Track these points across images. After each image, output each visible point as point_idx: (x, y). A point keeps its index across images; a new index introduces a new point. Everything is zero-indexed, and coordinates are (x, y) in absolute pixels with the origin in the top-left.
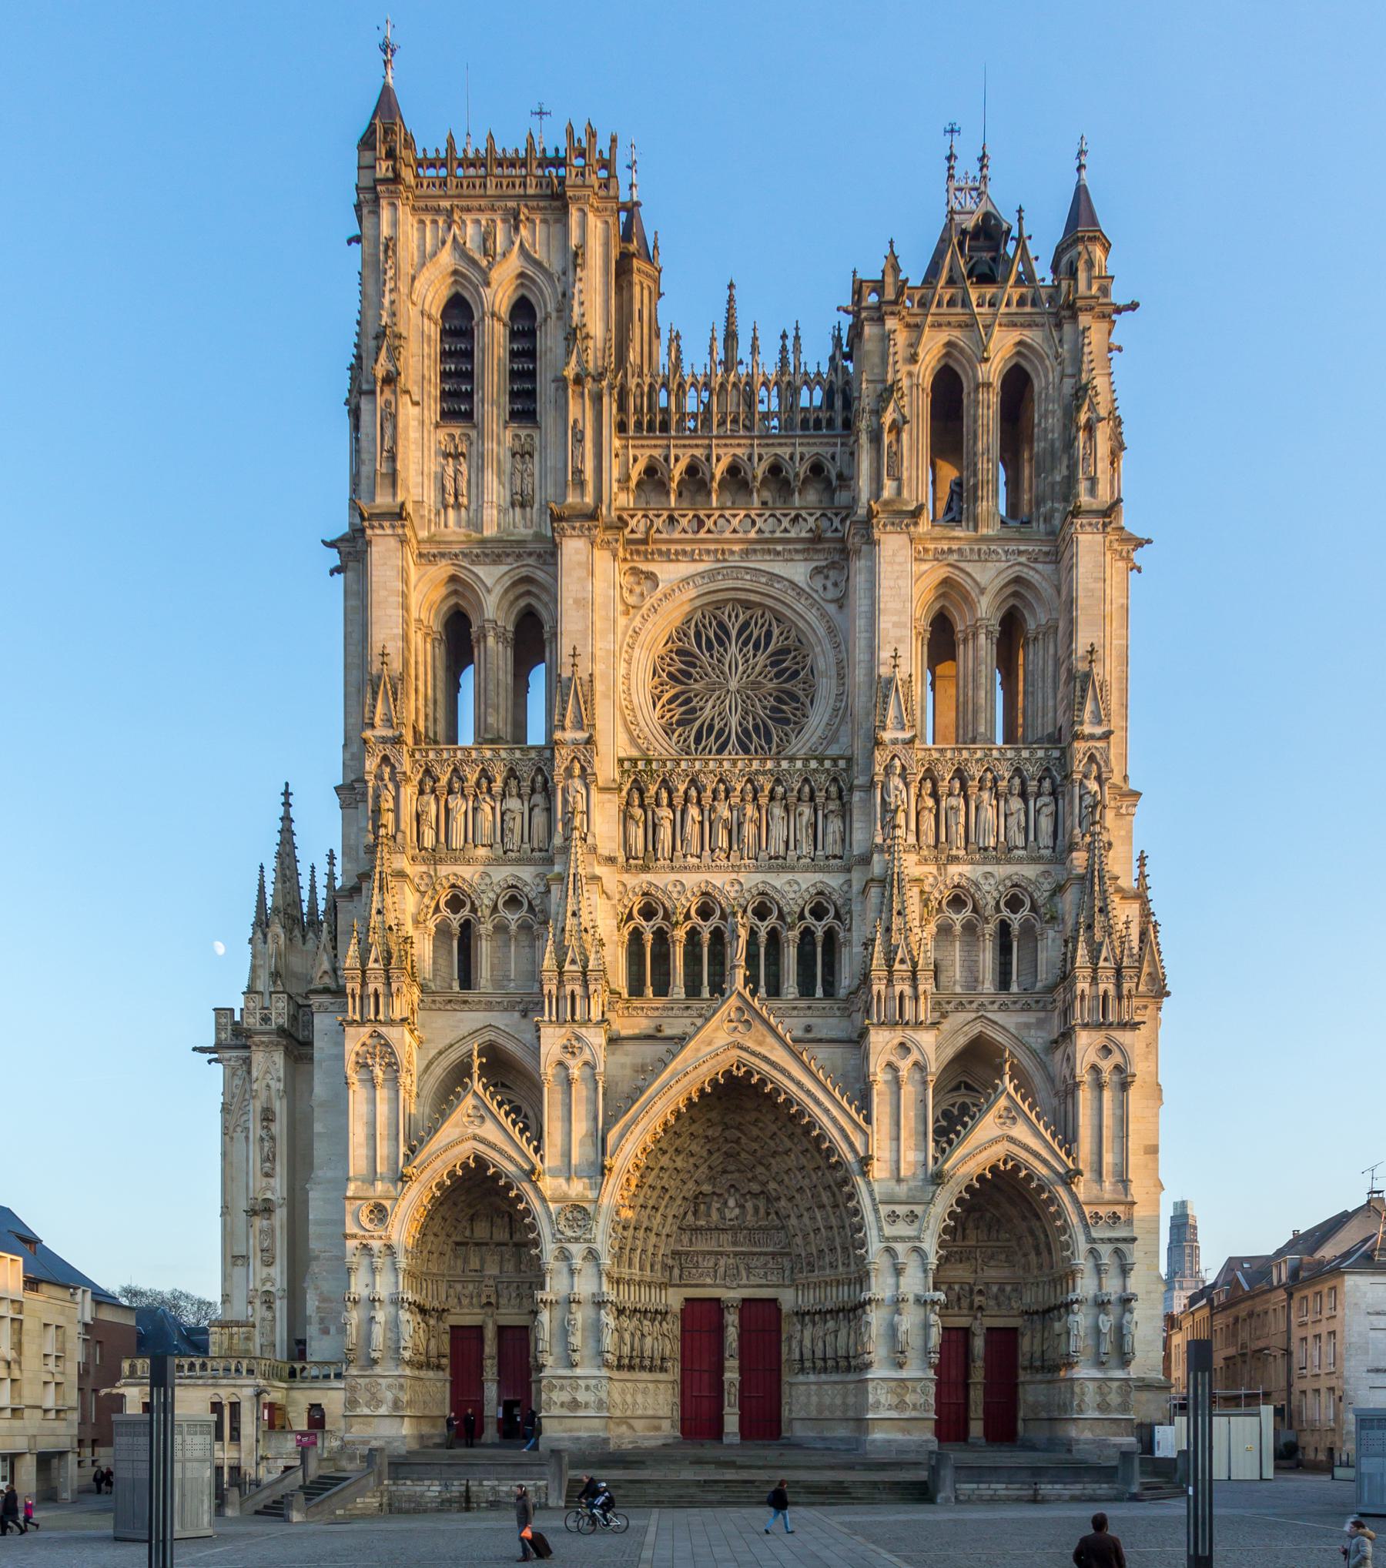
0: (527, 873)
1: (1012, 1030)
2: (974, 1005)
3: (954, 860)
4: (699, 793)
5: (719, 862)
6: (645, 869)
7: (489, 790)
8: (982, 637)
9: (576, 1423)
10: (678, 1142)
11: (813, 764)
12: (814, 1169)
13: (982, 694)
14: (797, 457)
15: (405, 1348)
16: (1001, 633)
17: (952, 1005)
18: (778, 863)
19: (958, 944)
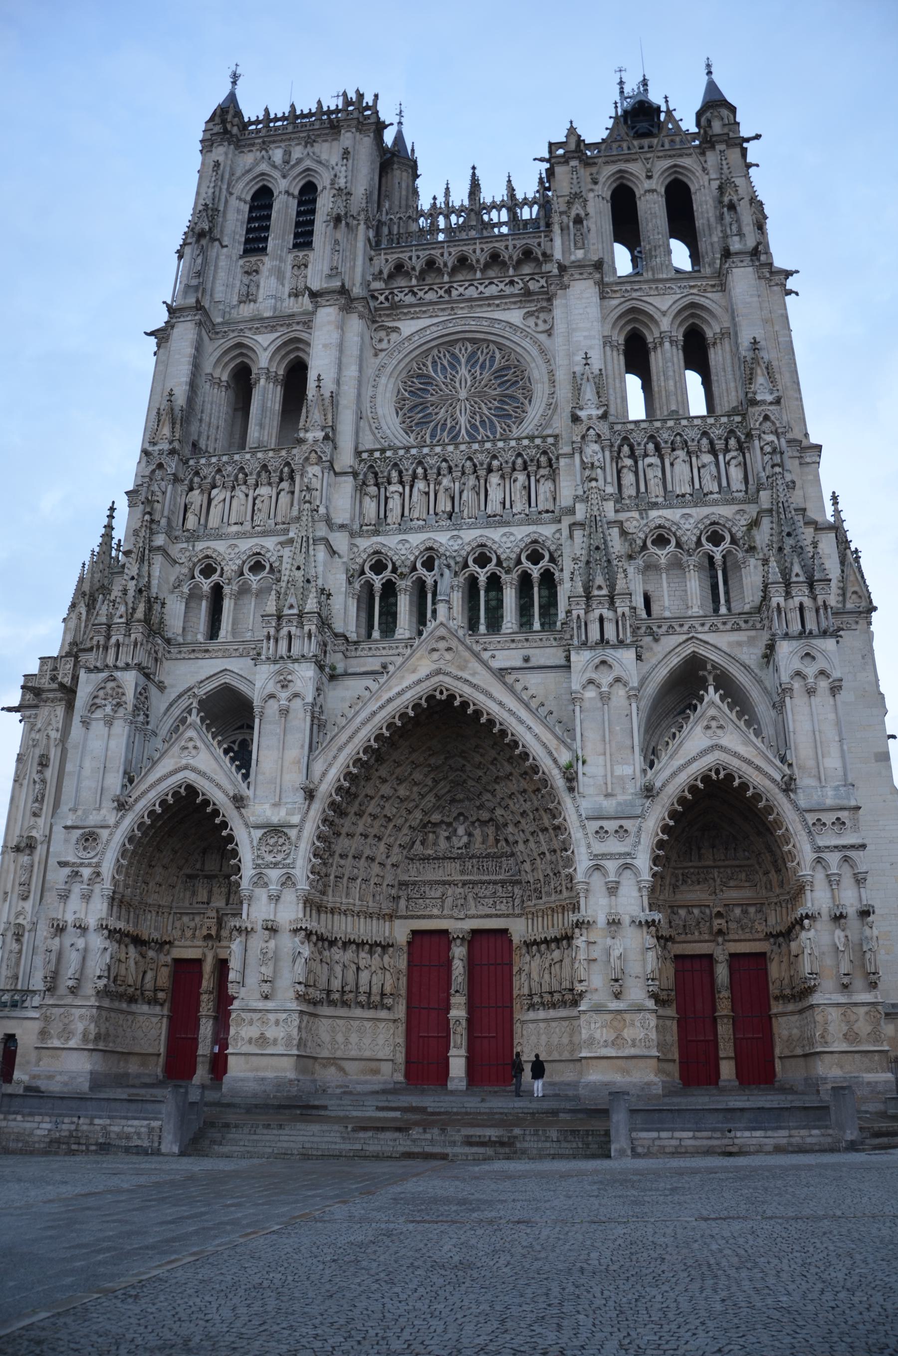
0: (270, 543)
1: (725, 648)
2: (686, 628)
3: (655, 506)
4: (425, 470)
5: (441, 523)
6: (377, 533)
7: (245, 482)
8: (667, 345)
9: (264, 1061)
10: (398, 771)
11: (526, 442)
12: (534, 792)
13: (671, 383)
14: (510, 248)
15: (99, 977)
16: (685, 341)
17: (664, 628)
18: (494, 520)
19: (664, 575)
